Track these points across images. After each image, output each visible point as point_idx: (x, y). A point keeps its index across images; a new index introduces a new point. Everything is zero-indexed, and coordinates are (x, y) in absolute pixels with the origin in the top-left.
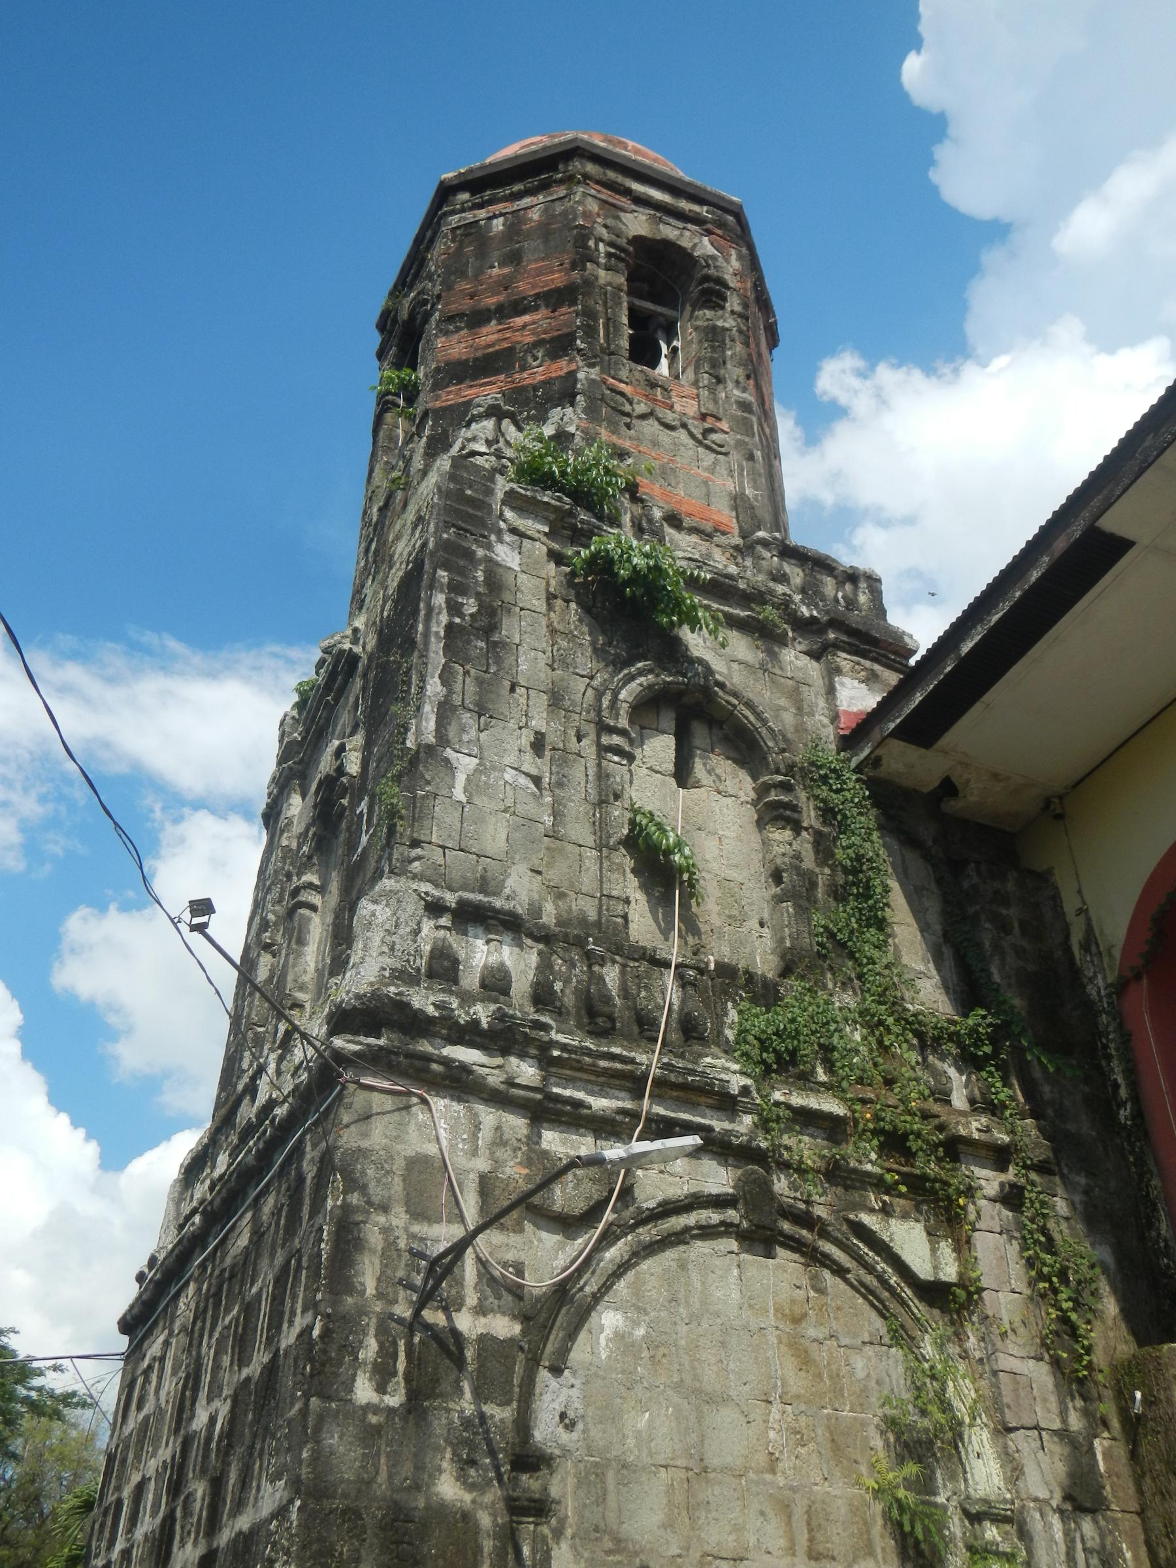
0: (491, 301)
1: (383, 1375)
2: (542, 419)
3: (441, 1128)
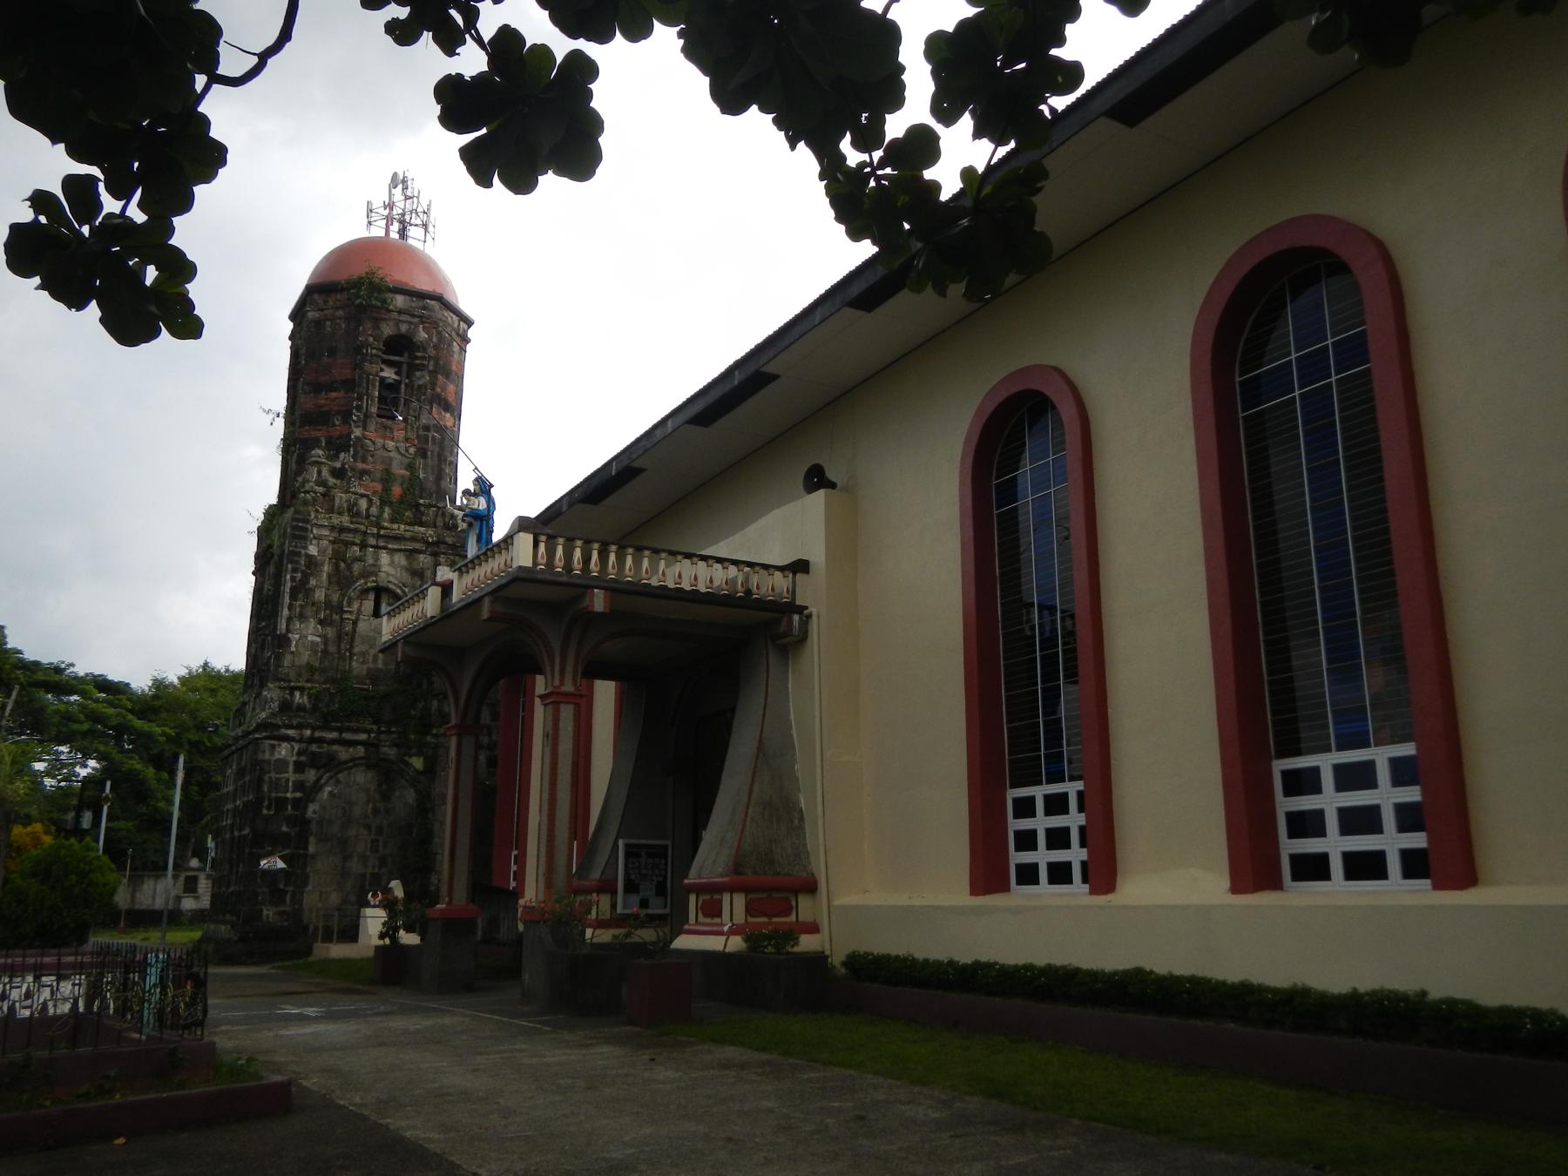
0: (323, 379)
1: (269, 808)
2: (336, 457)
3: (283, 750)
